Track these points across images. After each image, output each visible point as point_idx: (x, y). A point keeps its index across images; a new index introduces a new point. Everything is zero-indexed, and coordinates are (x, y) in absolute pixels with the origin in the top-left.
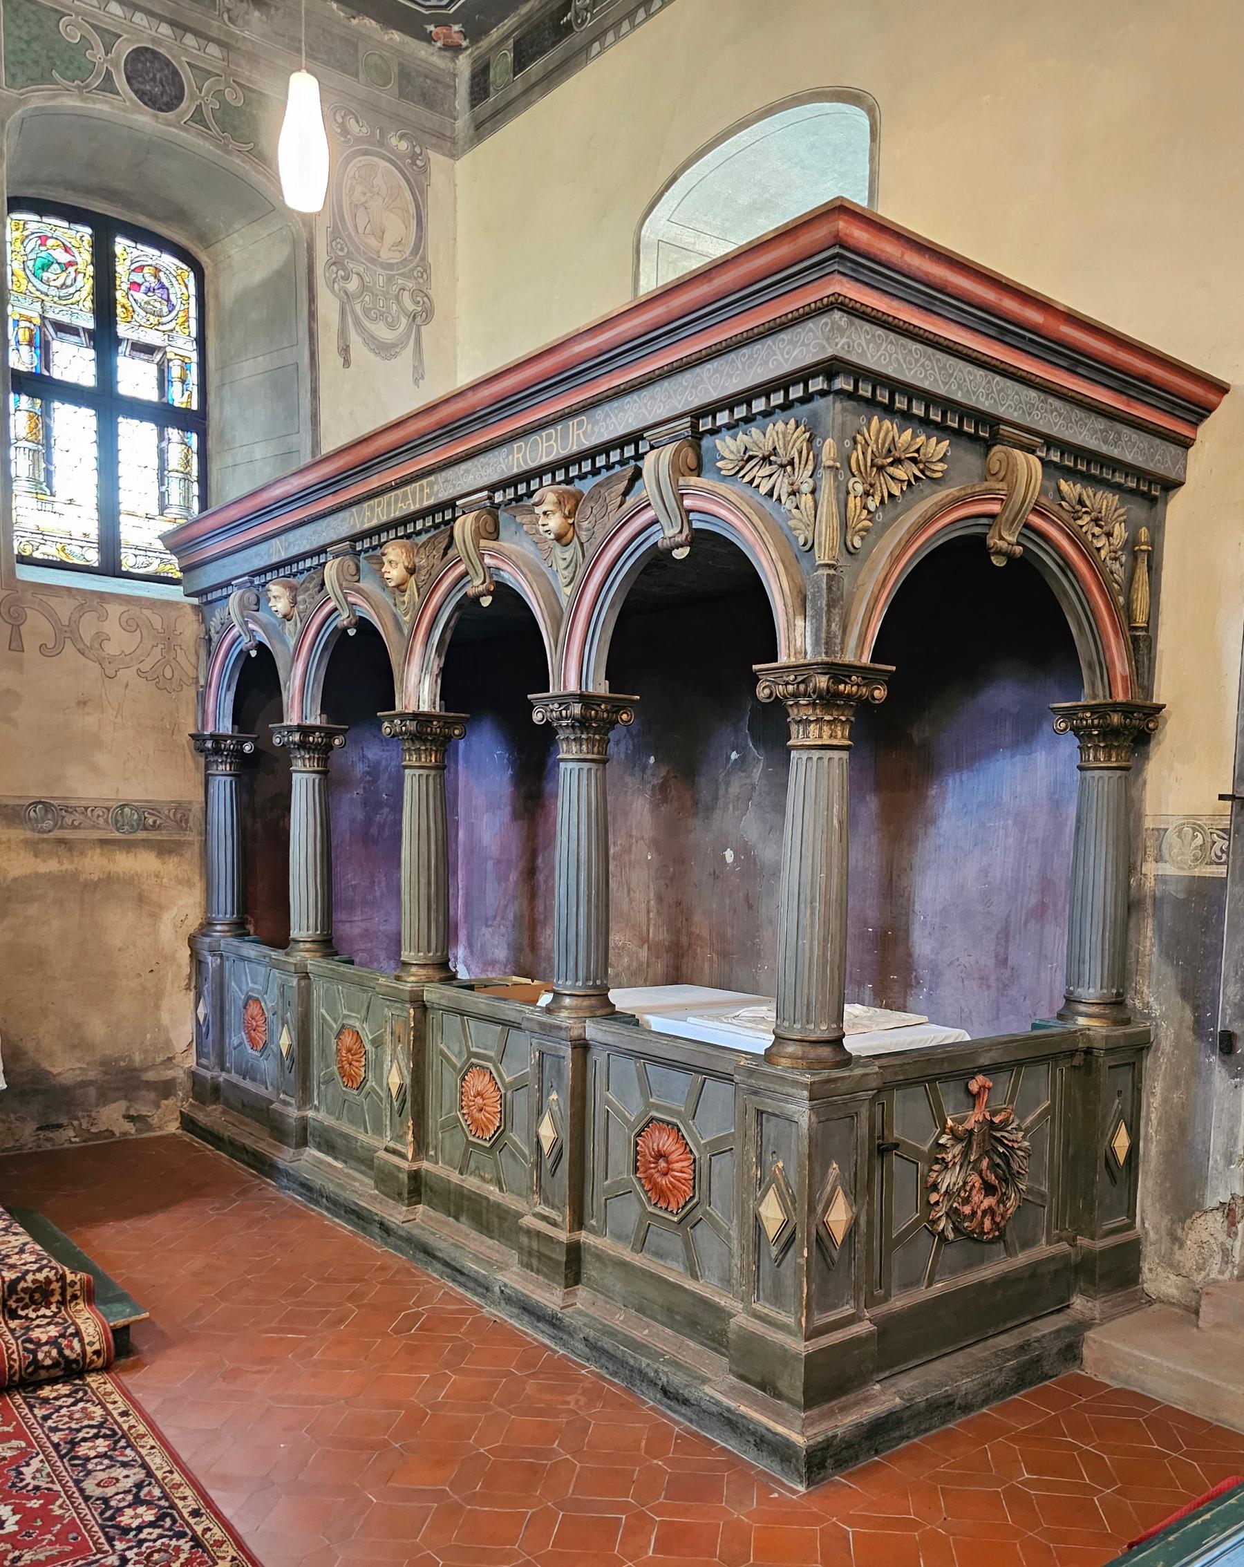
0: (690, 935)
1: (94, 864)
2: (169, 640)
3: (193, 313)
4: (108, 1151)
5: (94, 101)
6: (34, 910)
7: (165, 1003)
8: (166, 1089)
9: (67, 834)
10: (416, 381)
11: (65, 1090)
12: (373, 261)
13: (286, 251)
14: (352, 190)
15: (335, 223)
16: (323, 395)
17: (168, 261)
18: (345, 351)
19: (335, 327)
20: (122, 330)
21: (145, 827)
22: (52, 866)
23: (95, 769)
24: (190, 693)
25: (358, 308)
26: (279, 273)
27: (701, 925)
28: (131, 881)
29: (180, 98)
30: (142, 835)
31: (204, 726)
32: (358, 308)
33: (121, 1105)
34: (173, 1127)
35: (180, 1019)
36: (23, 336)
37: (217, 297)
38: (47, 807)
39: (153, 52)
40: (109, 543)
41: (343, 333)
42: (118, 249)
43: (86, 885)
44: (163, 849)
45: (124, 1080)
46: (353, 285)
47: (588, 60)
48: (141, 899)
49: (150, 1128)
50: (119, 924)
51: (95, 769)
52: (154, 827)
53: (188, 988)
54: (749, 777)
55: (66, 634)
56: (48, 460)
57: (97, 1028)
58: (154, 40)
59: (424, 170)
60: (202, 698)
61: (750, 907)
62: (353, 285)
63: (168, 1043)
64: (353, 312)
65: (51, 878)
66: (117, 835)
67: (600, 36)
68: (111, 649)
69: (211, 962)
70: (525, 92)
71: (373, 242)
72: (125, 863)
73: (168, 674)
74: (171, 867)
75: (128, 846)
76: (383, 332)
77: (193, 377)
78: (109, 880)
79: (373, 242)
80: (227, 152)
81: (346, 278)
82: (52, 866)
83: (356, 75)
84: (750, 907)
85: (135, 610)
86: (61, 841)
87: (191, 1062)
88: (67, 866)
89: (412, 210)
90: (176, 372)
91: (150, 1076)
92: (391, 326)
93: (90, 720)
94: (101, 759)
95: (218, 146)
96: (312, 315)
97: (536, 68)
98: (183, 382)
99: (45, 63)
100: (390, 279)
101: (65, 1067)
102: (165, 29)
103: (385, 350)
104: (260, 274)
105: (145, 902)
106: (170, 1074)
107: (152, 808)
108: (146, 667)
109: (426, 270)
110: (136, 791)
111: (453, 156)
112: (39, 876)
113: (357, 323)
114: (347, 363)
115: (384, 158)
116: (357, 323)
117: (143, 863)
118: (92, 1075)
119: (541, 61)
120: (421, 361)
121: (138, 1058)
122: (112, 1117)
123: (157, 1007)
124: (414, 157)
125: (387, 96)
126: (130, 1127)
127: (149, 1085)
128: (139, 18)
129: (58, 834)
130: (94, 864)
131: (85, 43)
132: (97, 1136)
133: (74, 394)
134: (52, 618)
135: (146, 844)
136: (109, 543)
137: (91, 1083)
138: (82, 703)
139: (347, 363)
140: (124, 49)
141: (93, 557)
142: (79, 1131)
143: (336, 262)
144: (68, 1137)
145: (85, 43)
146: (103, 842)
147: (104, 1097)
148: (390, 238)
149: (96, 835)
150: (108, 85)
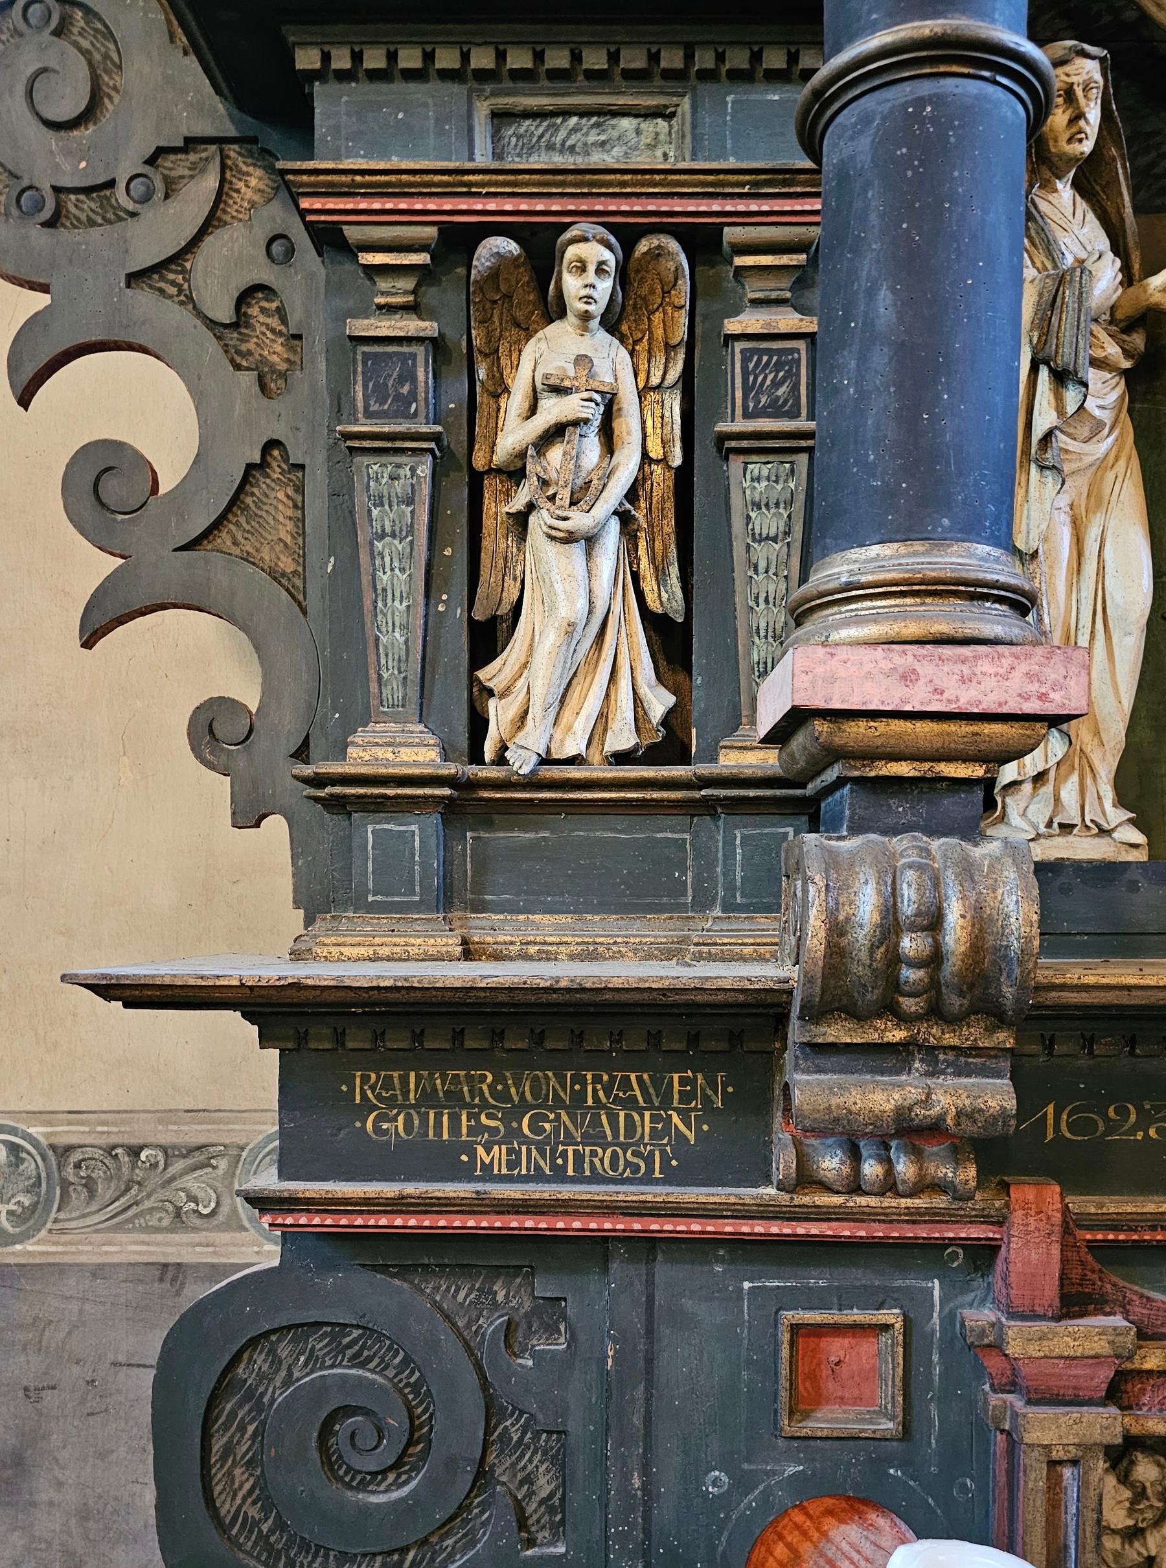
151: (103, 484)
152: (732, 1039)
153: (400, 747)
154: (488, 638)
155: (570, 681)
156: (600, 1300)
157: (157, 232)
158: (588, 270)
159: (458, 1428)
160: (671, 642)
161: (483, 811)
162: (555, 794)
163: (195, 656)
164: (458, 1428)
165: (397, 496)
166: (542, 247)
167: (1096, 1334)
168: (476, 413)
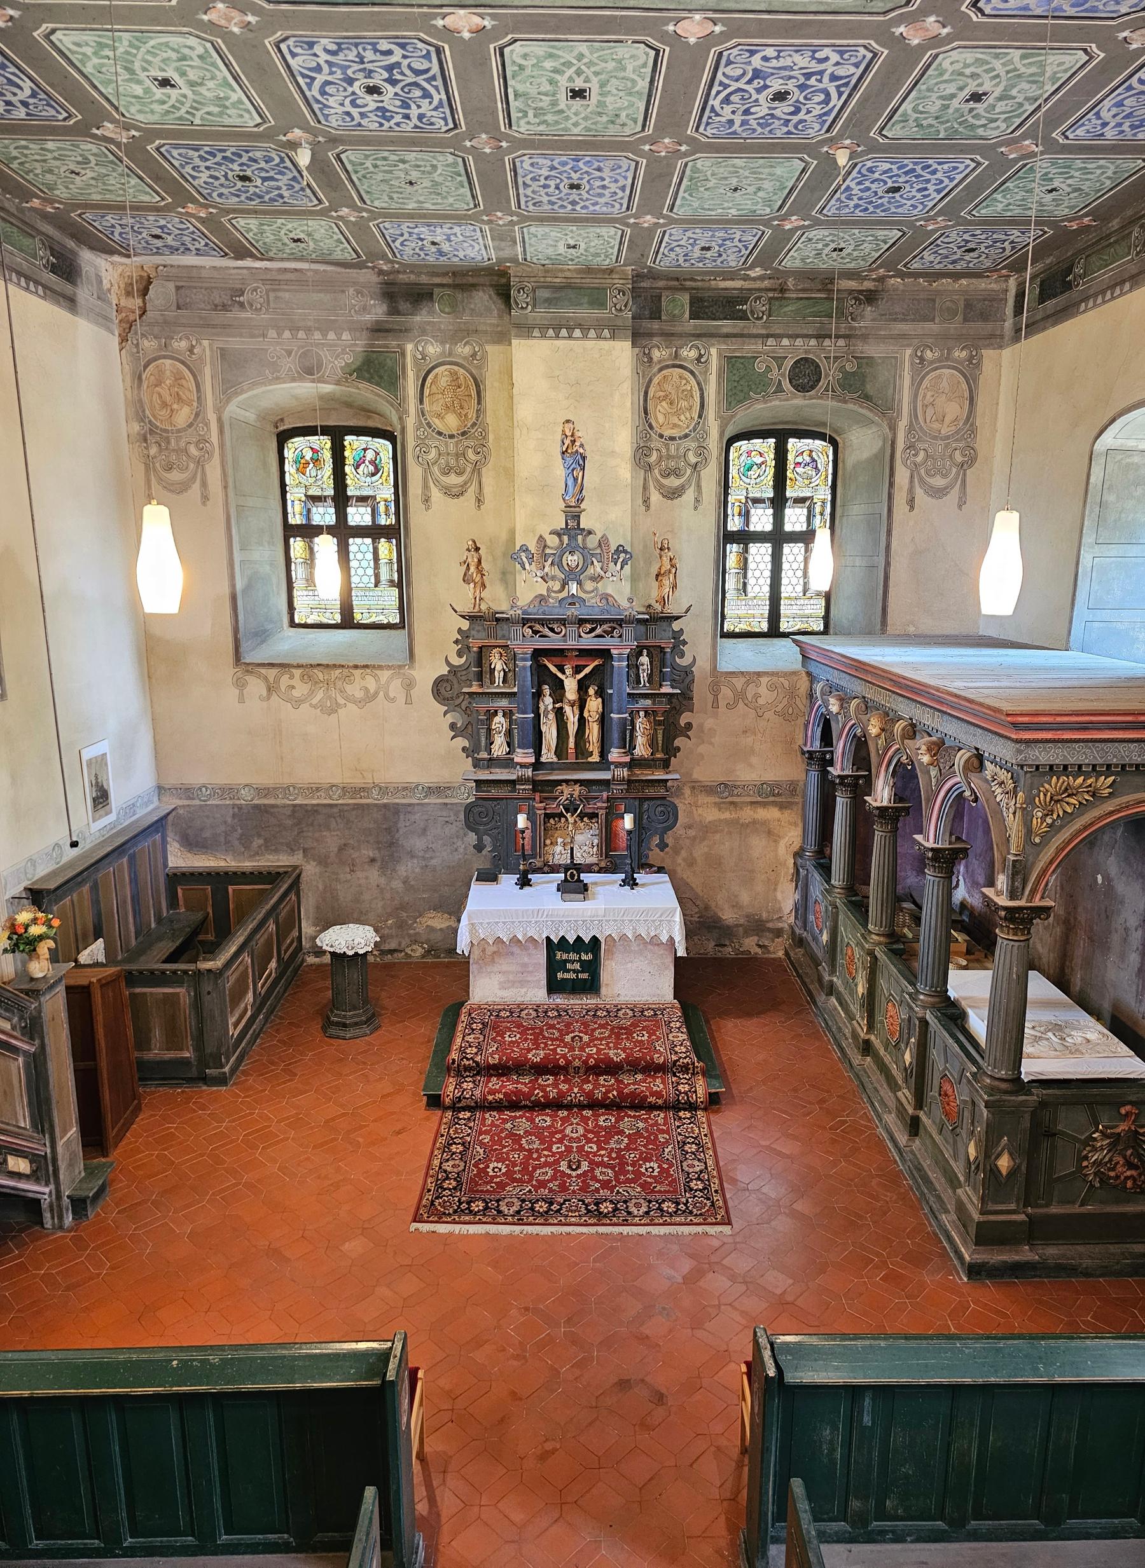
0: (1076, 919)
1: (747, 814)
2: (792, 693)
3: (830, 471)
4: (747, 964)
5: (771, 401)
6: (717, 836)
7: (779, 888)
8: (778, 933)
9: (735, 799)
10: (960, 507)
11: (728, 927)
12: (935, 438)
13: (881, 443)
14: (924, 397)
15: (911, 421)
16: (894, 533)
17: (818, 443)
18: (911, 503)
19: (906, 487)
20: (788, 494)
21: (775, 794)
22: (727, 815)
23: (751, 765)
24: (801, 721)
25: (922, 472)
26: (876, 456)
27: (1082, 917)
28: (764, 823)
29: (819, 380)
30: (771, 799)
31: (805, 745)
32: (922, 472)
33: (756, 938)
34: (781, 954)
35: (787, 898)
36: (736, 510)
37: (843, 462)
38: (726, 786)
39: (806, 359)
40: (774, 616)
41: (911, 490)
42: (790, 446)
43: (742, 825)
44: (782, 807)
45: (758, 926)
46: (920, 458)
47: (1078, 313)
48: (769, 833)
49: (769, 952)
50: (758, 844)
51: (751, 765)
52: (779, 794)
53: (792, 881)
54: (1115, 833)
55: (740, 696)
56: (745, 577)
57: (745, 898)
58: (806, 352)
59: (978, 365)
60: (806, 726)
61: (1107, 917)
62: (920, 458)
63: (780, 909)
64: (919, 475)
65: (727, 822)
66: (759, 799)
67: (1086, 299)
68: (761, 701)
69: (802, 872)
70: (1043, 319)
71: (936, 426)
72: (762, 814)
73: (790, 711)
74: (787, 816)
75: (764, 805)
76: (938, 482)
77: (828, 510)
78: (754, 822)
79: (936, 426)
80: (845, 402)
81: (915, 455)
82: (727, 815)
83: (933, 320)
84: (1107, 917)
85: (775, 679)
86: (732, 803)
87: (792, 920)
88: (734, 816)
89: (967, 394)
90: (818, 509)
91: (770, 925)
92: (944, 476)
93: (749, 740)
94: (754, 760)
95: (840, 401)
96: (891, 484)
97: (1051, 304)
98: (822, 514)
99: (746, 389)
100: (946, 446)
101: (728, 916)
102: (813, 342)
103: (938, 493)
104: (866, 454)
105: (772, 835)
106: (780, 925)
107: (778, 784)
108: (778, 709)
109: (973, 431)
110: (770, 776)
111: (1001, 347)
112: (720, 820)
113: (921, 480)
114: (912, 508)
115: (949, 367)
116: (921, 480)
117: (771, 814)
118: (742, 921)
119: (1054, 301)
120: (965, 493)
121: (764, 915)
122: (750, 944)
123: (775, 890)
124: (972, 357)
125: (955, 326)
126: (759, 951)
127: (770, 930)
128: (799, 342)
129: (730, 799)
130: (747, 814)
131: (769, 369)
132: (742, 953)
133: (760, 537)
134: (733, 689)
135: (774, 804)
136: (774, 616)
137: (741, 925)
138: (745, 732)
139: (912, 508)
140: (789, 364)
141: (765, 626)
142: (734, 949)
143: (910, 447)
144: (729, 952)
145: (769, 369)
146: (752, 803)
147: (747, 933)
148: (947, 420)
149: (749, 799)
150: (780, 389)
151: (453, 726)
152: (513, 783)
153: (484, 755)
154: (492, 743)
155: (499, 747)
156: (501, 802)
157: (457, 702)
158: (500, 714)
159: (491, 814)
160: (509, 745)
161: (492, 762)
162: (498, 759)
163: (462, 742)
164: (491, 814)
165: (483, 732)
166: (496, 711)
167: (543, 805)
168: (490, 725)
